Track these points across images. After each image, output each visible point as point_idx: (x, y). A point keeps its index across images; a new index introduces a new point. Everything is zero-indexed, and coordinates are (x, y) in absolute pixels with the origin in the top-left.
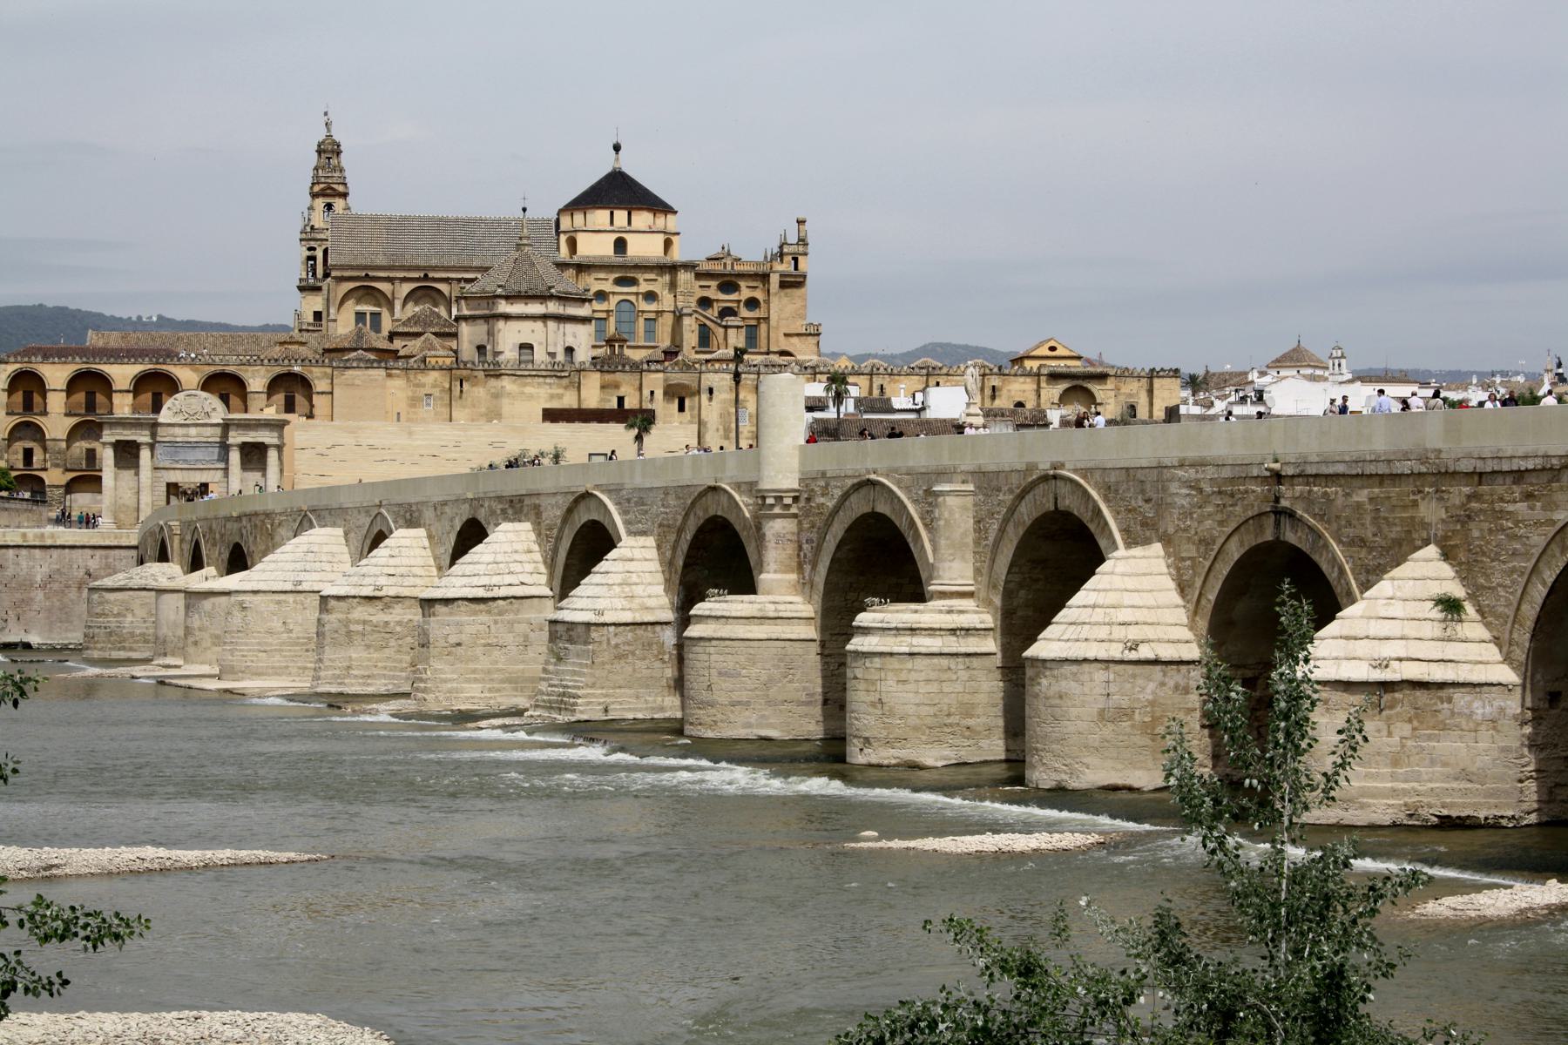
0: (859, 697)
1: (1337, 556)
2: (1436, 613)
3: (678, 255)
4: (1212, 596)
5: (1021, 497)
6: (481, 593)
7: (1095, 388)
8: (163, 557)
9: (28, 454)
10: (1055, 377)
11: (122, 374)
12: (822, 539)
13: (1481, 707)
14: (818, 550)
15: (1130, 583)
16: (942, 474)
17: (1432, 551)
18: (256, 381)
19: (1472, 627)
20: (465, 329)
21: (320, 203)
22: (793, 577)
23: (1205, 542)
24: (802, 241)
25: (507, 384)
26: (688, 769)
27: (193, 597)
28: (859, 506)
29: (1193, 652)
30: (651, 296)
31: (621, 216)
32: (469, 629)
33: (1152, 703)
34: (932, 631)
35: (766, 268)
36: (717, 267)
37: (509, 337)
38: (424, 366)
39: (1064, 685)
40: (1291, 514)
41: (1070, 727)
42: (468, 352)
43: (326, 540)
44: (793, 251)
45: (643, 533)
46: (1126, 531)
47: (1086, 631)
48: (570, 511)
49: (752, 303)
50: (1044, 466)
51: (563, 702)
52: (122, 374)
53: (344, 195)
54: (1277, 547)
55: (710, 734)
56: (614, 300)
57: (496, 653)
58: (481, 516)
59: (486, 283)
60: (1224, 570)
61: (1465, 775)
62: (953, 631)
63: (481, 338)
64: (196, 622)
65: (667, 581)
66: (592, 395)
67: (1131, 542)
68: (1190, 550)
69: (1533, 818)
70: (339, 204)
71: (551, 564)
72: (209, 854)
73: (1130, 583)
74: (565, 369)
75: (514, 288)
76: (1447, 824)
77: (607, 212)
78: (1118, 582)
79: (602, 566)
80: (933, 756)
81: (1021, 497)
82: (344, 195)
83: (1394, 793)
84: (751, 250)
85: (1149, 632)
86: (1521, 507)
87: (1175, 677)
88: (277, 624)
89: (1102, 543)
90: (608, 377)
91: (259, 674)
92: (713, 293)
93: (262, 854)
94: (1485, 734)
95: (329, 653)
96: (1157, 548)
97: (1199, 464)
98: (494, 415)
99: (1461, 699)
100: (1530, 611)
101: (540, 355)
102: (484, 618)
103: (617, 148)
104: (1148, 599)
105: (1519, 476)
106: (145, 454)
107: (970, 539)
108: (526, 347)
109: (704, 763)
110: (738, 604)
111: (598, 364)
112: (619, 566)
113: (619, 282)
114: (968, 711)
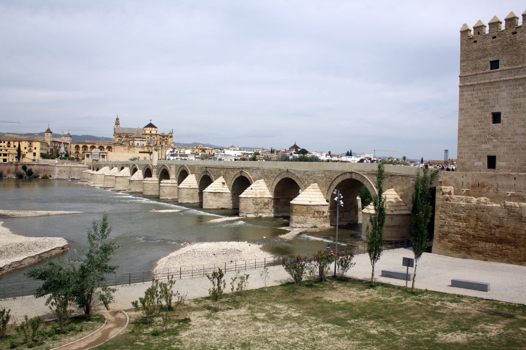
0: (161, 191)
1: (212, 177)
2: (222, 184)
3: (157, 133)
4: (200, 181)
5: (180, 168)
6: (122, 176)
7: (205, 150)
8: (90, 169)
9: (77, 155)
10: (201, 149)
11: (89, 146)
12: (159, 171)
13: (226, 195)
14: (159, 173)
15: (190, 179)
16: (172, 165)
17: (222, 177)
18: (105, 147)
19: (226, 186)
20: (131, 141)
21: (116, 125)
22: (156, 176)
23: (199, 174)
24: (172, 132)
25: (135, 148)
26: (140, 199)
27: (92, 174)
28: (163, 168)
29: (198, 187)
30: (154, 138)
31: (151, 128)
32: (121, 180)
33: (192, 193)
34: (169, 183)
37: (136, 143)
38: (126, 146)
39: (182, 191)
40: (208, 172)
41: (183, 196)
42: (131, 144)
43: (107, 168)
44: (171, 133)
45: (140, 169)
46: (191, 172)
47: (185, 185)
48: (133, 166)
49: (166, 139)
50: (183, 164)
51: (130, 190)
52: (89, 146)
53: (119, 124)
54: (206, 175)
55: (146, 194)
57: (124, 183)
58: (124, 166)
59: (134, 136)
60: (201, 178)
61: (224, 203)
62: (172, 183)
63: (133, 143)
64: (92, 177)
65: (143, 175)
66: (146, 150)
67: (191, 174)
68: (197, 175)
69: (232, 208)
70: (118, 125)
71: (131, 172)
72: (70, 212)
73: (190, 179)
74: (143, 147)
75: (137, 137)
76: (222, 209)
77: (149, 128)
78: (189, 179)
79: (135, 173)
80: (169, 198)
81: (180, 168)
82: (119, 124)
83: (216, 205)
84: (166, 133)
85: (192, 185)
86: (231, 172)
87: (195, 190)
88: (100, 178)
89: (188, 174)
91: (98, 184)
92: (162, 138)
93: (77, 212)
94: (226, 198)
95: (105, 182)
96: (194, 175)
97: (199, 165)
98: (134, 152)
99: (224, 194)
100: (232, 184)
101: (140, 145)
102: (122, 179)
103: (151, 120)
104: (192, 181)
105: (231, 169)
106: (90, 156)
107: (175, 172)
108: (138, 144)
109: (143, 198)
110: (149, 179)
111: (147, 146)
112: (137, 173)
113: (150, 136)
114: (173, 193)
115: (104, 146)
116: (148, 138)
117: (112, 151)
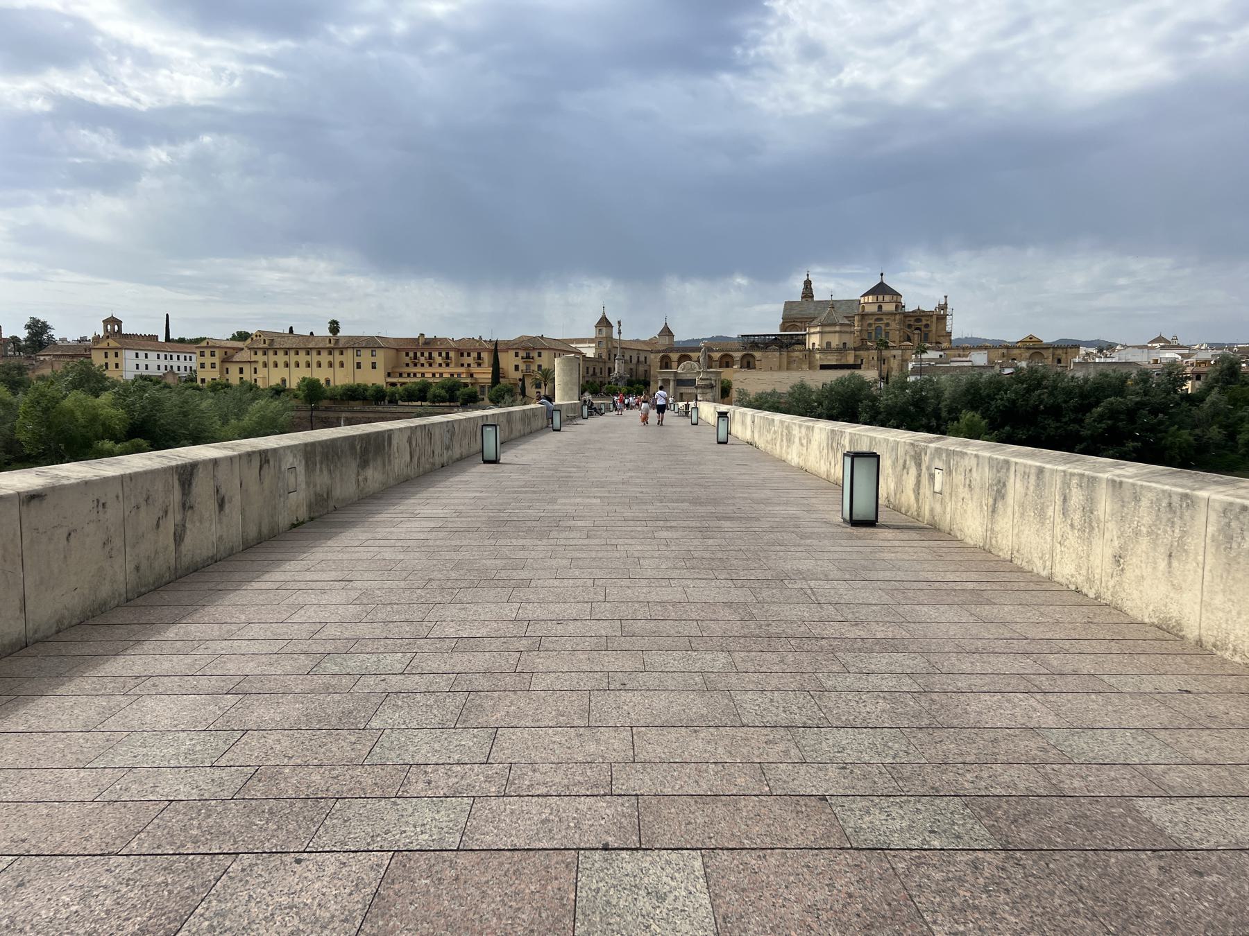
10: (1028, 348)
18: (737, 355)
21: (804, 300)
24: (946, 304)
30: (888, 325)
31: (880, 298)
35: (931, 314)
36: (915, 314)
44: (944, 307)
49: (927, 326)
56: (873, 327)
82: (813, 297)
84: (929, 307)
90: (858, 353)
101: (834, 345)
103: (882, 275)
106: (672, 383)
113: (877, 320)
115: (735, 354)
116: (870, 325)
117: (755, 368)
